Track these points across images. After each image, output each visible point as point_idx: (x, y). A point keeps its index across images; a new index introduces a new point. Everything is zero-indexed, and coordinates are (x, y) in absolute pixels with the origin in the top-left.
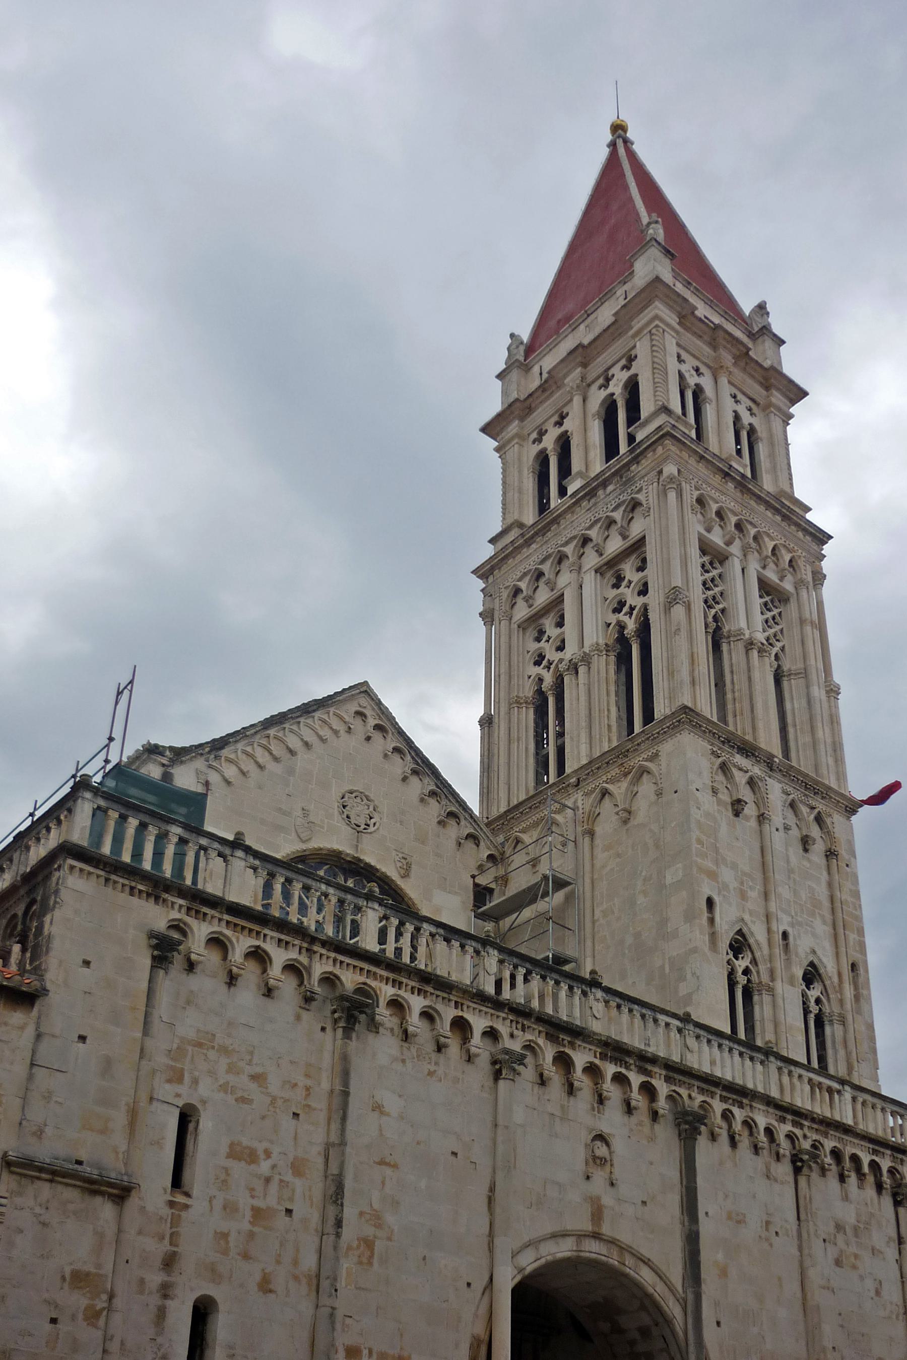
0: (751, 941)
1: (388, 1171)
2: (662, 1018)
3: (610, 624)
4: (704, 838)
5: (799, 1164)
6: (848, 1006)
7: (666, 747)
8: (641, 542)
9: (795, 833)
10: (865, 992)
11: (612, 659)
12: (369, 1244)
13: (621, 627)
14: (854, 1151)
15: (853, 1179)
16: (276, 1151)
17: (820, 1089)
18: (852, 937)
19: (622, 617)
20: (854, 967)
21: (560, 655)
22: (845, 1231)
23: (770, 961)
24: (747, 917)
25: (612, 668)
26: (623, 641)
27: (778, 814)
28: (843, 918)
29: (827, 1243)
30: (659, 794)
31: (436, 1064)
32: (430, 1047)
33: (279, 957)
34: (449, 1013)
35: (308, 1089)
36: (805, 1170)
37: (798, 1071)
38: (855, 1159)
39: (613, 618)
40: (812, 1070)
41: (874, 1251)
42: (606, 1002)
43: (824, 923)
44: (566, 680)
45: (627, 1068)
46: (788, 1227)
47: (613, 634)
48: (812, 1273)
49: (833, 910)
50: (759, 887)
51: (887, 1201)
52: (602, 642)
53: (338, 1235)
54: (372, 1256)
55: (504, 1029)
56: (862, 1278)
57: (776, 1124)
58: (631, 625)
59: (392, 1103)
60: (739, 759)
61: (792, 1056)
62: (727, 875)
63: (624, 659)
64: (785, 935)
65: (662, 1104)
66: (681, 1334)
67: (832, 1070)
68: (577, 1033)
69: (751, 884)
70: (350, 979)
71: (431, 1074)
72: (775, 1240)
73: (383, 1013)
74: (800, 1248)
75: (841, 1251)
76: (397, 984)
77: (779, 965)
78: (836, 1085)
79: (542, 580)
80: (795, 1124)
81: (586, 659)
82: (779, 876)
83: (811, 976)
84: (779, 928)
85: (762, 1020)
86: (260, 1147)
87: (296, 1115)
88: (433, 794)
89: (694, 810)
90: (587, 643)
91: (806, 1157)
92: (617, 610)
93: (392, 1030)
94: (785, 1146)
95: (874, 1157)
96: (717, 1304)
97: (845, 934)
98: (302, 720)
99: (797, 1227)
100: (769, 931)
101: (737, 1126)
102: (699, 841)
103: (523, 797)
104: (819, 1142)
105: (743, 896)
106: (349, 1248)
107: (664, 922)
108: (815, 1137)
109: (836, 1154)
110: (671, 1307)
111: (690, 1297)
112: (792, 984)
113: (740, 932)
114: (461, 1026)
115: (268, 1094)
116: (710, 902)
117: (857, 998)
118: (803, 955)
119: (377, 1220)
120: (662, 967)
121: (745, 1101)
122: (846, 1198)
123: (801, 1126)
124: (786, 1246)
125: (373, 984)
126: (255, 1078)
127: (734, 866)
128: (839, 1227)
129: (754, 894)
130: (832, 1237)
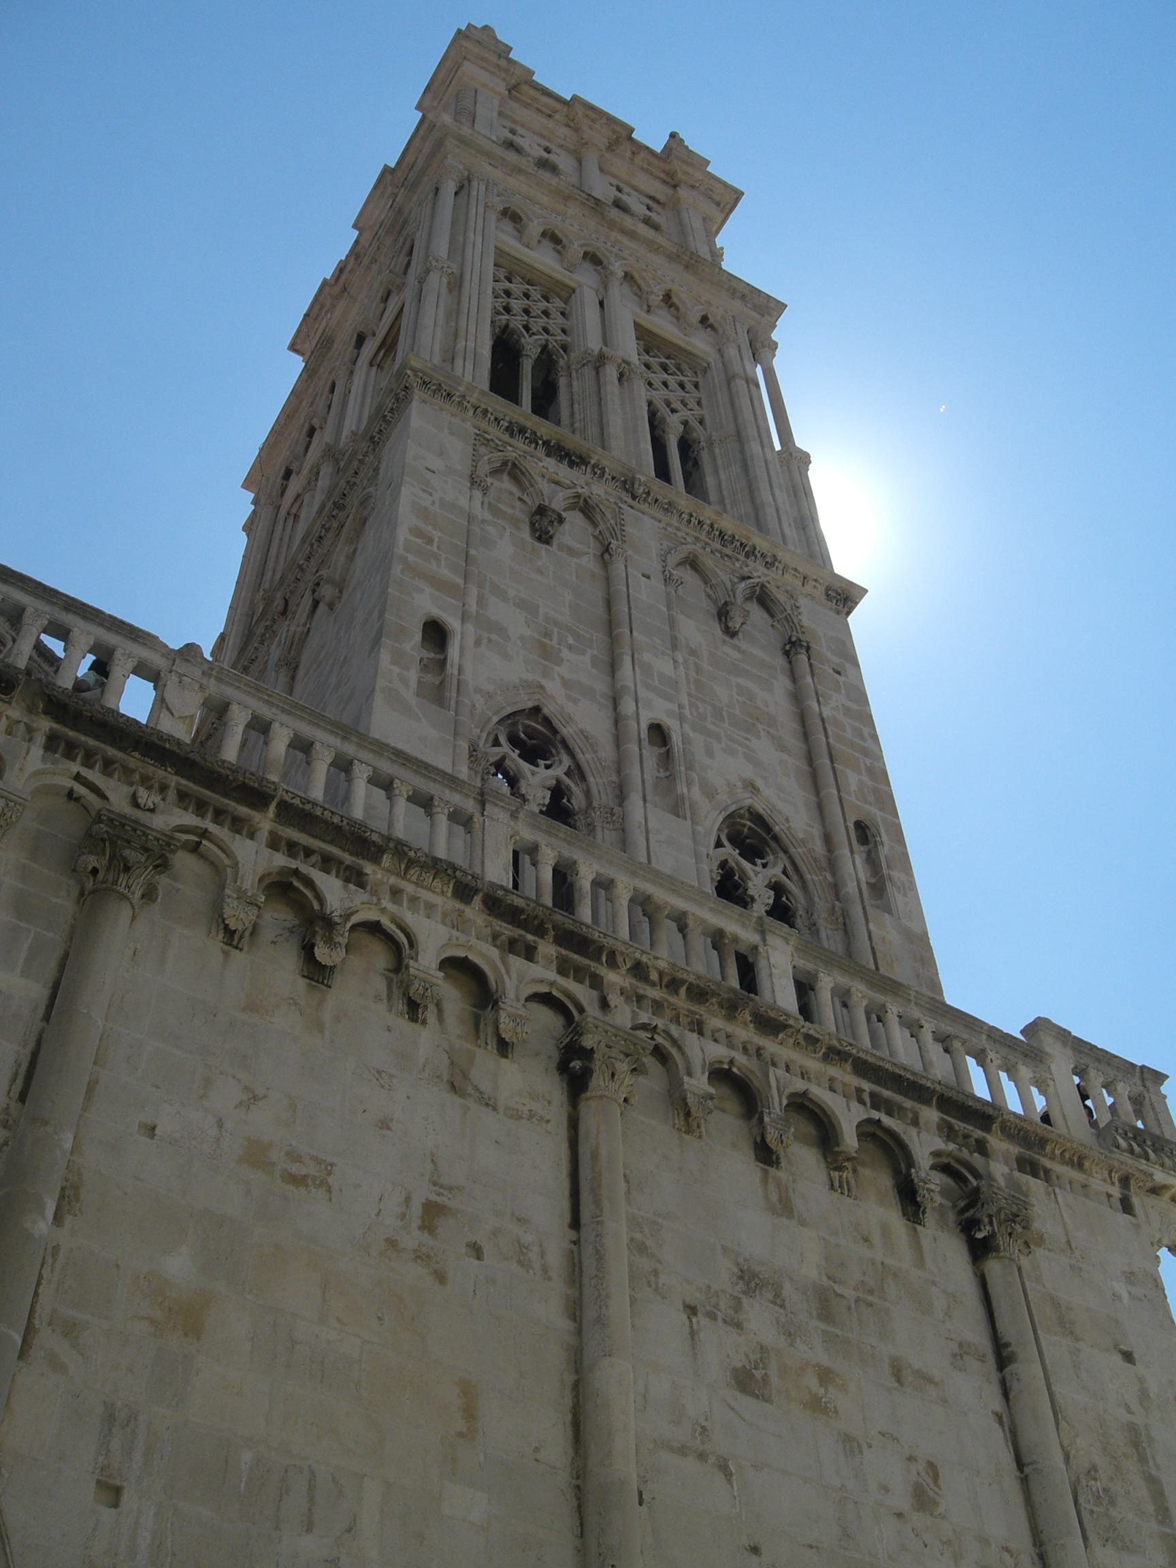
0: (566, 731)
5: (576, 1064)
10: (896, 874)
14: (799, 1085)
17: (682, 928)
20: (864, 832)
22: (777, 1295)
23: (619, 772)
24: (553, 687)
28: (828, 743)
29: (701, 1320)
36: (598, 1082)
46: (528, 1238)
57: (494, 953)
64: (659, 733)
69: (571, 640)
74: (575, 1310)
75: (763, 1349)
95: (876, 1115)
97: (834, 769)
102: (417, 532)
104: (667, 1033)
105: (547, 654)
117: (878, 888)
121: (369, 868)
122: (784, 1207)
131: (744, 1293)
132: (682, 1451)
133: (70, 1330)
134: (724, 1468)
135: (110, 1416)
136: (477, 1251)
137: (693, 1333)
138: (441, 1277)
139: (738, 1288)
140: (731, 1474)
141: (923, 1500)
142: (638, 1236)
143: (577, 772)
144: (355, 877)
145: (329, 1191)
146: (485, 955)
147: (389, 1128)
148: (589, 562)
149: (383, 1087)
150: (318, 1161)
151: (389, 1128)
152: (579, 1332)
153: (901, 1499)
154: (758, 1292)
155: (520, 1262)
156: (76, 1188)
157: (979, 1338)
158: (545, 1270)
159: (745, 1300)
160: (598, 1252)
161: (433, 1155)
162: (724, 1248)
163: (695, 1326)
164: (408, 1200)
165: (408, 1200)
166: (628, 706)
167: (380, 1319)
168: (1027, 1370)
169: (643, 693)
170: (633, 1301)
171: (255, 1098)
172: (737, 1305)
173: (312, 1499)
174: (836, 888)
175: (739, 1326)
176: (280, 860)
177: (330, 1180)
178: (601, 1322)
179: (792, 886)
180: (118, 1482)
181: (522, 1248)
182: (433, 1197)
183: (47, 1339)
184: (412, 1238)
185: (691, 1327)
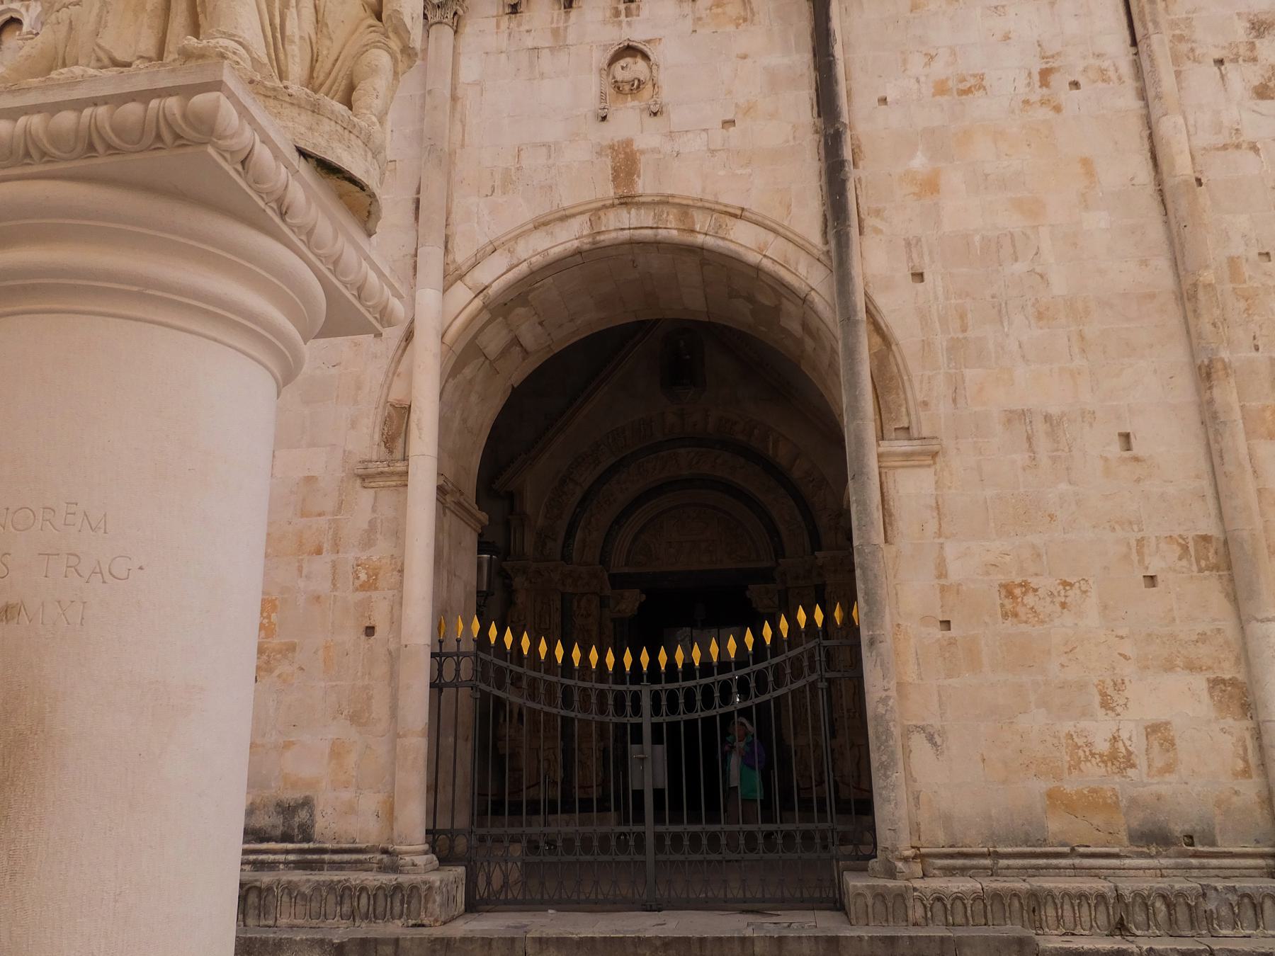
29: (1227, 64)
46: (1106, 64)
48: (1171, 127)
74: (1142, 94)
99: (1131, 57)
110: (802, 270)
130: (1243, 50)
131: (1257, 37)
132: (1225, 147)
133: (878, 213)
134: (1254, 148)
135: (908, 244)
136: (1075, 85)
137: (1222, 76)
138: (1057, 109)
139: (1251, 36)
140: (1259, 150)
142: (1178, 32)
145: (985, 89)
147: (1009, 38)
149: (1000, 15)
150: (974, 76)
151: (1009, 38)
152: (1147, 106)
154: (1266, 33)
155: (1104, 80)
156: (859, 147)
158: (1120, 78)
159: (1257, 42)
160: (1149, 56)
161: (1038, 42)
162: (1239, 14)
163: (1224, 72)
164: (1030, 74)
165: (1030, 74)
167: (1029, 145)
170: (1178, 74)
171: (932, 58)
172: (1252, 46)
173: (1014, 246)
175: (1255, 60)
177: (984, 83)
178: (1159, 97)
180: (921, 271)
181: (1102, 71)
182: (1044, 66)
183: (870, 222)
184: (1038, 93)
185: (1221, 73)
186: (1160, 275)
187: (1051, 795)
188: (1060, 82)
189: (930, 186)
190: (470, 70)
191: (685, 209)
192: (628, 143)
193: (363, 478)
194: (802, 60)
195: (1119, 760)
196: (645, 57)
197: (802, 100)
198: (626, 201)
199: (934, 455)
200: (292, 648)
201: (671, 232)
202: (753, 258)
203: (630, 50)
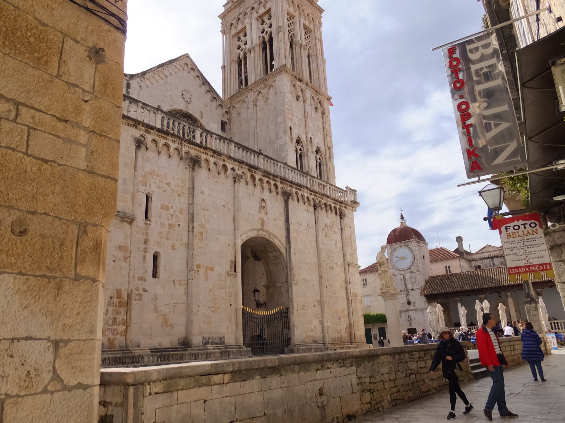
0: (302, 140)
1: (206, 212)
2: (279, 164)
3: (260, 37)
4: (289, 108)
6: (328, 159)
7: (278, 78)
8: (270, 10)
9: (313, 107)
11: (261, 48)
12: (201, 234)
13: (264, 38)
15: (329, 211)
16: (174, 206)
18: (329, 139)
19: (264, 35)
21: (245, 46)
24: (300, 133)
25: (261, 52)
26: (264, 42)
27: (309, 101)
30: (276, 93)
31: (218, 179)
32: (216, 174)
33: (173, 146)
34: (222, 163)
35: (182, 187)
36: (317, 209)
37: (315, 180)
38: (330, 205)
39: (261, 35)
40: (318, 179)
41: (335, 232)
42: (264, 159)
43: (321, 134)
44: (248, 55)
45: (270, 179)
47: (261, 39)
49: (324, 131)
50: (304, 123)
51: (338, 217)
52: (258, 43)
53: (193, 232)
54: (202, 238)
55: (236, 168)
56: (332, 240)
58: (267, 38)
59: (206, 191)
60: (298, 83)
61: (313, 175)
62: (295, 119)
63: (264, 49)
64: (311, 138)
65: (280, 190)
66: (285, 258)
67: (323, 179)
68: (256, 168)
70: (193, 153)
71: (217, 182)
72: (309, 230)
73: (203, 163)
74: (316, 232)
76: (206, 154)
77: (309, 147)
78: (325, 184)
79: (240, 21)
80: (315, 196)
81: (254, 48)
82: (309, 120)
83: (317, 151)
84: (310, 136)
85: (305, 164)
86: (170, 206)
87: (179, 195)
88: (209, 91)
89: (286, 99)
90: (254, 43)
91: (317, 205)
92: (262, 32)
93: (205, 168)
94: (312, 202)
96: (294, 249)
98: (169, 65)
100: (307, 137)
101: (300, 196)
102: (288, 109)
103: (235, 93)
106: (196, 235)
107: (277, 134)
108: (320, 199)
109: (325, 204)
111: (288, 247)
112: (313, 153)
113: (299, 137)
114: (224, 166)
115: (171, 189)
116: (291, 128)
117: (330, 157)
118: (315, 144)
119: (203, 226)
120: (277, 148)
122: (328, 217)
123: (316, 196)
124: (312, 231)
125: (200, 154)
126: (167, 184)
127: (297, 117)
128: (326, 226)
129: (302, 126)
141: (336, 244)
143: (302, 146)
144: (300, 190)
146: (309, 196)
148: (302, 103)
153: (334, 244)
157: (340, 228)
166: (308, 136)
168: (343, 231)
169: (310, 132)
174: (326, 159)
176: (296, 190)
179: (321, 158)
186: (316, 261)
187: (306, 336)
188: (309, 226)
189: (296, 240)
190: (241, 194)
191: (269, 234)
192: (263, 218)
193: (229, 274)
194: (282, 211)
195: (312, 331)
196: (265, 202)
197: (283, 219)
198: (262, 230)
199: (297, 284)
200: (220, 307)
201: (267, 237)
202: (277, 245)
203: (263, 200)
